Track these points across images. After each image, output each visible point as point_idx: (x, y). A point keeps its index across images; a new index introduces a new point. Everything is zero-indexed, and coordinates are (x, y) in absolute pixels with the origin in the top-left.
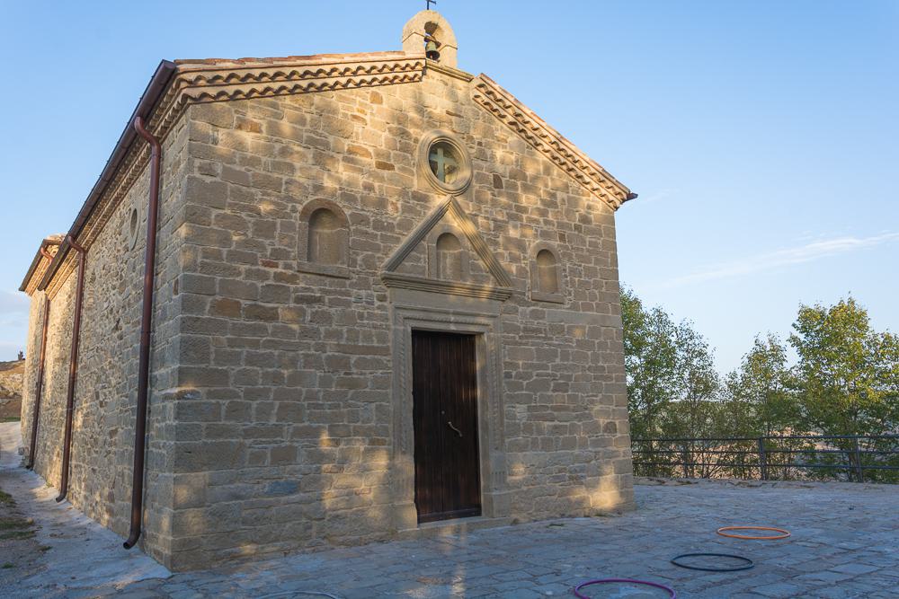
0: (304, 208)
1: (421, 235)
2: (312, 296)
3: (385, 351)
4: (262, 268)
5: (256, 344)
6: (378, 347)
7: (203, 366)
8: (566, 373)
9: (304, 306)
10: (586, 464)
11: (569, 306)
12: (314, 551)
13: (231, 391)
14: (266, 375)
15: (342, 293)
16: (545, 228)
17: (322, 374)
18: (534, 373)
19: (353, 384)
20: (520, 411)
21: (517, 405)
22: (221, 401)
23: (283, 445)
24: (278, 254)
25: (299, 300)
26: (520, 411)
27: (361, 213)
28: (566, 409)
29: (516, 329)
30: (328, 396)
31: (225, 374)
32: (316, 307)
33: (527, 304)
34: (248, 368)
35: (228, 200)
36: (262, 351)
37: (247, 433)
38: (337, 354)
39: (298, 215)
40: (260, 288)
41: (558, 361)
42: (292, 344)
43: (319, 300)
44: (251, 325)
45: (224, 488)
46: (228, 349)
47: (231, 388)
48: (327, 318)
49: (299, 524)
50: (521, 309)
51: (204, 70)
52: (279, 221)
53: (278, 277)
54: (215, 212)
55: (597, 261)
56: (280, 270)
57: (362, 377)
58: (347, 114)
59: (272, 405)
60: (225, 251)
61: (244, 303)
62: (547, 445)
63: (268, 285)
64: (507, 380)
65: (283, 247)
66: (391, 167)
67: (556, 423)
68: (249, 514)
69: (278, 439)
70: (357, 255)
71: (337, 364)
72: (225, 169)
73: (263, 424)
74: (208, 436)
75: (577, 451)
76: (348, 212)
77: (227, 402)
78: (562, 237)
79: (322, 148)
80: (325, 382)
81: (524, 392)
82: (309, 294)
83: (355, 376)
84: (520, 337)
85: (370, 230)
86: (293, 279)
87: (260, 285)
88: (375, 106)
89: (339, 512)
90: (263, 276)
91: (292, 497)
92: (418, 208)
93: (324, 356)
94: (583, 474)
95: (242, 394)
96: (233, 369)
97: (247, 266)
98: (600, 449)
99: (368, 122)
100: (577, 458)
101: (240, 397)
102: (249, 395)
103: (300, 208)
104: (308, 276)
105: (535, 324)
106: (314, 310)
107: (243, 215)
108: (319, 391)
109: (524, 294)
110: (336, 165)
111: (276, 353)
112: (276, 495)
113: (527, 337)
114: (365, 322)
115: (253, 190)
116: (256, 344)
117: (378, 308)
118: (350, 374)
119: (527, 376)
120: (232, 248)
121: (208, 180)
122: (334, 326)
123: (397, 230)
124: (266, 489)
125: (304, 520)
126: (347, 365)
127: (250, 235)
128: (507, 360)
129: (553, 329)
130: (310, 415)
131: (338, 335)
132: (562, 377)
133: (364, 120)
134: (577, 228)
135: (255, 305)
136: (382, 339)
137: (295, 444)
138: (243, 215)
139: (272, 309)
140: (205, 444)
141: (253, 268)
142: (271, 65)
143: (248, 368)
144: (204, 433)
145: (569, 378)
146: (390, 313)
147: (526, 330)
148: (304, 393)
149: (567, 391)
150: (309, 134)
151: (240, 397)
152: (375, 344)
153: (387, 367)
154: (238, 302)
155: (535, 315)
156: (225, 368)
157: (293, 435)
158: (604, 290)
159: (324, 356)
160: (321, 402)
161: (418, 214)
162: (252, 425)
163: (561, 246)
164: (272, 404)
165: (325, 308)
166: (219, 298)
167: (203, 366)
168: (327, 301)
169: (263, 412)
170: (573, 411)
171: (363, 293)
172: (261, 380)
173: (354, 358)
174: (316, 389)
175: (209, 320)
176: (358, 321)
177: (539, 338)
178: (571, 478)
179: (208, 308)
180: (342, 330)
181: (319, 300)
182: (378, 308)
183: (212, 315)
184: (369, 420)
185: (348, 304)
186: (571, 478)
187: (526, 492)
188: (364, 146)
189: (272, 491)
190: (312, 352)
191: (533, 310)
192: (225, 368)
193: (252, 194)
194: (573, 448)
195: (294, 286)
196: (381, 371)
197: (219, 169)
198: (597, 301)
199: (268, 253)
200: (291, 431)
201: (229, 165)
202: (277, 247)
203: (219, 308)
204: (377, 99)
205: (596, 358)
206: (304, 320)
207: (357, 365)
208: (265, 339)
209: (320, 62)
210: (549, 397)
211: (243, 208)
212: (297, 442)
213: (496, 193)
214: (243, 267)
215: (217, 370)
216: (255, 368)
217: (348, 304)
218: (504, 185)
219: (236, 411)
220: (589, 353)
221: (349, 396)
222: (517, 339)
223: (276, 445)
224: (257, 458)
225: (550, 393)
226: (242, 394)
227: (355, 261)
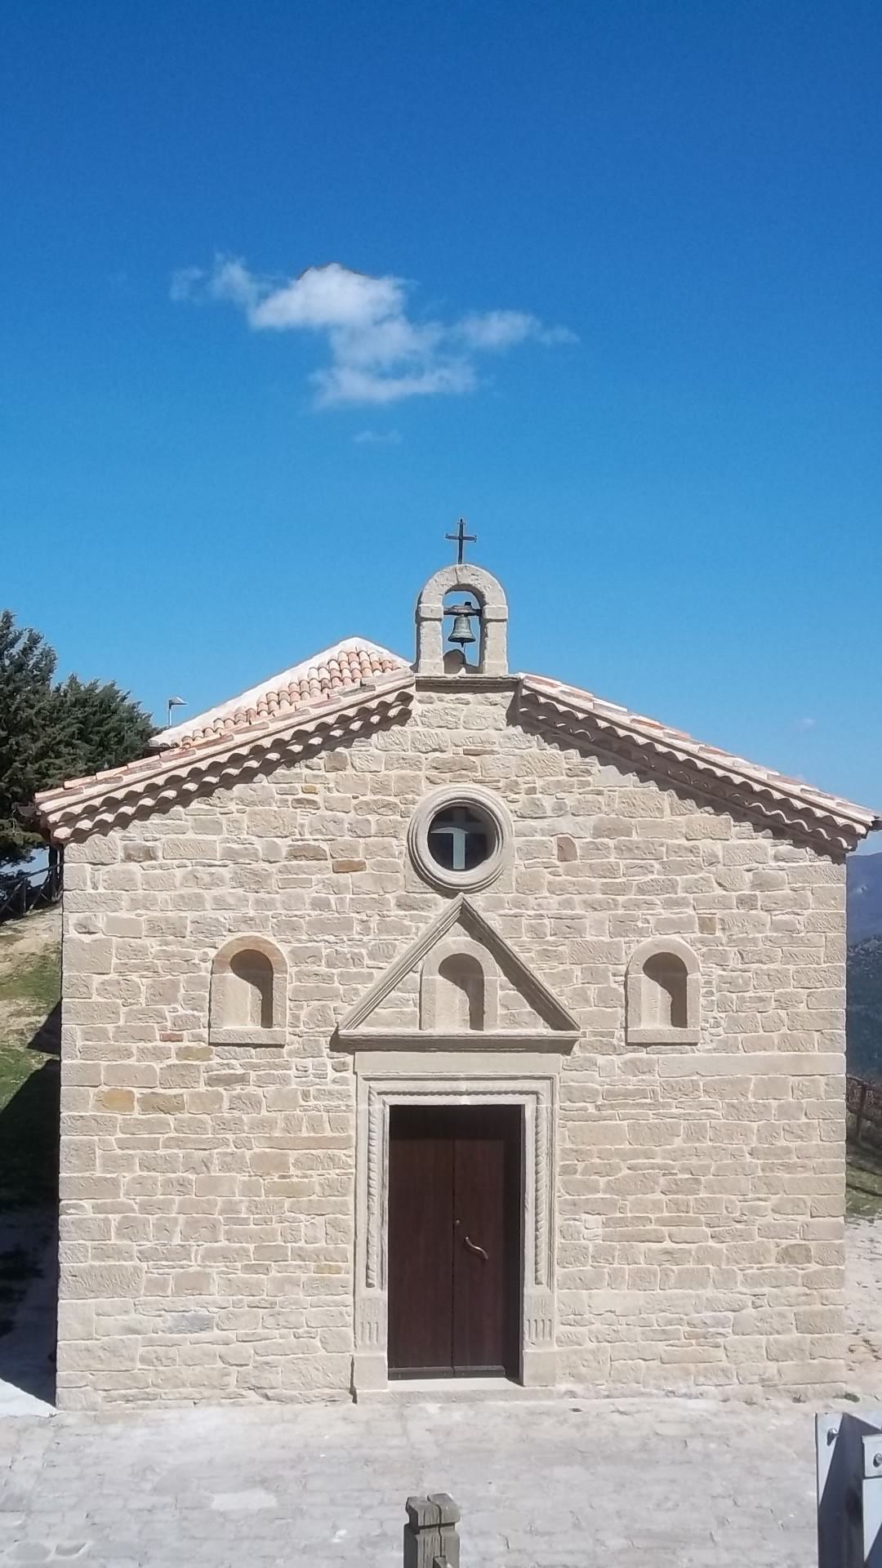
0: (217, 955)
1: (408, 966)
2: (232, 1075)
3: (343, 1144)
4: (162, 1044)
5: (153, 1145)
6: (333, 1138)
7: (87, 1174)
8: (694, 1161)
9: (221, 1089)
10: (730, 1315)
11: (714, 1045)
12: (232, 1403)
13: (123, 1204)
14: (169, 1183)
15: (277, 1066)
16: (666, 914)
17: (246, 1178)
18: (623, 1165)
19: (292, 1192)
20: (592, 1227)
21: (584, 1216)
22: (110, 1216)
23: (191, 1270)
24: (181, 1023)
25: (210, 1082)
26: (592, 1227)
27: (309, 944)
28: (695, 1222)
29: (589, 1095)
30: (254, 1208)
31: (115, 1183)
32: (238, 1089)
33: (615, 1050)
34: (145, 1174)
35: (114, 961)
36: (161, 1152)
37: (144, 1256)
38: (268, 1150)
39: (209, 965)
40: (158, 1071)
41: (678, 1142)
42: (202, 1141)
43: (242, 1079)
44: (148, 1120)
45: (116, 1320)
46: (119, 1152)
47: (122, 1199)
48: (254, 1103)
49: (213, 1369)
50: (601, 1060)
51: (70, 805)
52: (183, 977)
53: (185, 1053)
54: (97, 979)
55: (790, 958)
56: (185, 1043)
57: (306, 1180)
58: (287, 801)
59: (176, 1219)
60: (110, 1028)
61: (137, 1093)
62: (640, 1280)
63: (169, 1066)
64: (565, 1177)
65: (190, 1012)
66: (358, 867)
67: (668, 1244)
68: (148, 1352)
69: (184, 1262)
70: (302, 1007)
71: (263, 1165)
72: (112, 923)
73: (165, 1245)
74: (95, 1257)
75: (709, 1292)
76: (284, 950)
77: (118, 1217)
78: (706, 925)
79: (248, 861)
80: (249, 1189)
81: (600, 1195)
82: (228, 1071)
83: (295, 1180)
84: (598, 1108)
85: (323, 969)
86: (204, 1055)
87: (157, 1066)
88: (331, 775)
89: (268, 1359)
90: (159, 1054)
91: (203, 1335)
92: (407, 923)
93: (248, 1154)
94: (721, 1330)
95: (136, 1207)
96: (125, 1177)
97: (142, 1044)
98: (766, 1290)
99: (321, 804)
100: (711, 1305)
101: (133, 1211)
102: (145, 1208)
103: (212, 953)
104: (226, 1048)
105: (633, 1082)
106: (234, 1093)
107: (134, 977)
108: (242, 1201)
109: (612, 1034)
110: (269, 881)
111: (180, 1153)
112: (180, 1332)
113: (612, 1107)
114: (312, 1102)
115: (148, 942)
116: (153, 1145)
117: (334, 1081)
118: (289, 1177)
119: (610, 1170)
120: (121, 1023)
121: (87, 938)
122: (264, 1112)
123: (367, 961)
124: (169, 1324)
125: (220, 1364)
126: (282, 1165)
127: (142, 1000)
128: (569, 1145)
129: (670, 1088)
130: (227, 1232)
131: (269, 1124)
132: (683, 1170)
133: (313, 802)
134: (746, 902)
135: (153, 1093)
136: (339, 1125)
137: (208, 1270)
138: (134, 977)
139: (175, 1096)
140: (92, 1267)
141: (149, 1045)
142: (160, 770)
143: (145, 1174)
144: (90, 1255)
145: (705, 1170)
146: (352, 1089)
147: (609, 1095)
148: (219, 1203)
149: (695, 1192)
150: (224, 845)
151: (133, 1211)
152: (329, 1133)
153: (346, 1165)
154: (131, 1092)
155: (634, 1067)
156: (114, 1175)
157: (203, 1258)
158: (802, 1007)
159: (248, 1154)
160: (243, 1216)
161: (404, 931)
162: (149, 1244)
163: (703, 942)
164: (176, 1219)
165: (251, 1089)
166: (105, 1088)
167: (87, 1174)
168: (253, 1075)
169: (164, 1229)
170: (709, 1225)
171: (309, 1062)
172: (160, 1190)
173: (292, 1156)
174: (237, 1198)
175: (94, 1118)
176: (304, 1103)
177: (642, 1105)
178: (689, 1336)
179: (92, 1101)
180: (276, 1118)
181: (242, 1079)
182: (334, 1081)
183: (98, 1111)
184: (315, 1240)
185: (285, 1080)
186: (689, 1336)
187: (593, 1352)
188: (312, 843)
189: (177, 1326)
190: (232, 1149)
191: (632, 1062)
192: (114, 1175)
193: (145, 948)
194: (703, 1286)
195: (205, 1063)
196: (337, 1171)
197: (101, 923)
198: (785, 1030)
199: (169, 1024)
200: (201, 1252)
201: (114, 914)
202: (181, 1012)
203: (105, 1101)
204: (337, 766)
205: (770, 1133)
206: (220, 1107)
207: (298, 1163)
208: (166, 1136)
209: (230, 744)
210: (654, 1203)
211: (135, 969)
212: (211, 1267)
213: (561, 871)
214: (134, 1047)
215: (106, 1179)
216: (153, 1174)
217: (285, 1080)
218: (579, 852)
219: (129, 1228)
220: (755, 1125)
221: (286, 1206)
222: (591, 1109)
223: (181, 1270)
224: (158, 1286)
225: (658, 1196)
226: (136, 1207)
227: (296, 1018)
